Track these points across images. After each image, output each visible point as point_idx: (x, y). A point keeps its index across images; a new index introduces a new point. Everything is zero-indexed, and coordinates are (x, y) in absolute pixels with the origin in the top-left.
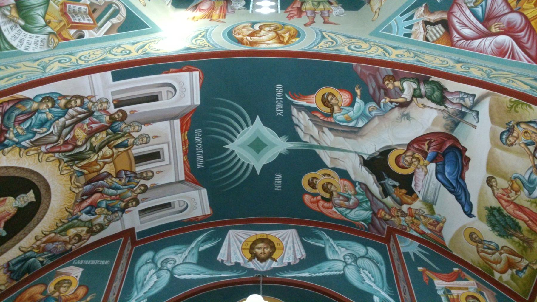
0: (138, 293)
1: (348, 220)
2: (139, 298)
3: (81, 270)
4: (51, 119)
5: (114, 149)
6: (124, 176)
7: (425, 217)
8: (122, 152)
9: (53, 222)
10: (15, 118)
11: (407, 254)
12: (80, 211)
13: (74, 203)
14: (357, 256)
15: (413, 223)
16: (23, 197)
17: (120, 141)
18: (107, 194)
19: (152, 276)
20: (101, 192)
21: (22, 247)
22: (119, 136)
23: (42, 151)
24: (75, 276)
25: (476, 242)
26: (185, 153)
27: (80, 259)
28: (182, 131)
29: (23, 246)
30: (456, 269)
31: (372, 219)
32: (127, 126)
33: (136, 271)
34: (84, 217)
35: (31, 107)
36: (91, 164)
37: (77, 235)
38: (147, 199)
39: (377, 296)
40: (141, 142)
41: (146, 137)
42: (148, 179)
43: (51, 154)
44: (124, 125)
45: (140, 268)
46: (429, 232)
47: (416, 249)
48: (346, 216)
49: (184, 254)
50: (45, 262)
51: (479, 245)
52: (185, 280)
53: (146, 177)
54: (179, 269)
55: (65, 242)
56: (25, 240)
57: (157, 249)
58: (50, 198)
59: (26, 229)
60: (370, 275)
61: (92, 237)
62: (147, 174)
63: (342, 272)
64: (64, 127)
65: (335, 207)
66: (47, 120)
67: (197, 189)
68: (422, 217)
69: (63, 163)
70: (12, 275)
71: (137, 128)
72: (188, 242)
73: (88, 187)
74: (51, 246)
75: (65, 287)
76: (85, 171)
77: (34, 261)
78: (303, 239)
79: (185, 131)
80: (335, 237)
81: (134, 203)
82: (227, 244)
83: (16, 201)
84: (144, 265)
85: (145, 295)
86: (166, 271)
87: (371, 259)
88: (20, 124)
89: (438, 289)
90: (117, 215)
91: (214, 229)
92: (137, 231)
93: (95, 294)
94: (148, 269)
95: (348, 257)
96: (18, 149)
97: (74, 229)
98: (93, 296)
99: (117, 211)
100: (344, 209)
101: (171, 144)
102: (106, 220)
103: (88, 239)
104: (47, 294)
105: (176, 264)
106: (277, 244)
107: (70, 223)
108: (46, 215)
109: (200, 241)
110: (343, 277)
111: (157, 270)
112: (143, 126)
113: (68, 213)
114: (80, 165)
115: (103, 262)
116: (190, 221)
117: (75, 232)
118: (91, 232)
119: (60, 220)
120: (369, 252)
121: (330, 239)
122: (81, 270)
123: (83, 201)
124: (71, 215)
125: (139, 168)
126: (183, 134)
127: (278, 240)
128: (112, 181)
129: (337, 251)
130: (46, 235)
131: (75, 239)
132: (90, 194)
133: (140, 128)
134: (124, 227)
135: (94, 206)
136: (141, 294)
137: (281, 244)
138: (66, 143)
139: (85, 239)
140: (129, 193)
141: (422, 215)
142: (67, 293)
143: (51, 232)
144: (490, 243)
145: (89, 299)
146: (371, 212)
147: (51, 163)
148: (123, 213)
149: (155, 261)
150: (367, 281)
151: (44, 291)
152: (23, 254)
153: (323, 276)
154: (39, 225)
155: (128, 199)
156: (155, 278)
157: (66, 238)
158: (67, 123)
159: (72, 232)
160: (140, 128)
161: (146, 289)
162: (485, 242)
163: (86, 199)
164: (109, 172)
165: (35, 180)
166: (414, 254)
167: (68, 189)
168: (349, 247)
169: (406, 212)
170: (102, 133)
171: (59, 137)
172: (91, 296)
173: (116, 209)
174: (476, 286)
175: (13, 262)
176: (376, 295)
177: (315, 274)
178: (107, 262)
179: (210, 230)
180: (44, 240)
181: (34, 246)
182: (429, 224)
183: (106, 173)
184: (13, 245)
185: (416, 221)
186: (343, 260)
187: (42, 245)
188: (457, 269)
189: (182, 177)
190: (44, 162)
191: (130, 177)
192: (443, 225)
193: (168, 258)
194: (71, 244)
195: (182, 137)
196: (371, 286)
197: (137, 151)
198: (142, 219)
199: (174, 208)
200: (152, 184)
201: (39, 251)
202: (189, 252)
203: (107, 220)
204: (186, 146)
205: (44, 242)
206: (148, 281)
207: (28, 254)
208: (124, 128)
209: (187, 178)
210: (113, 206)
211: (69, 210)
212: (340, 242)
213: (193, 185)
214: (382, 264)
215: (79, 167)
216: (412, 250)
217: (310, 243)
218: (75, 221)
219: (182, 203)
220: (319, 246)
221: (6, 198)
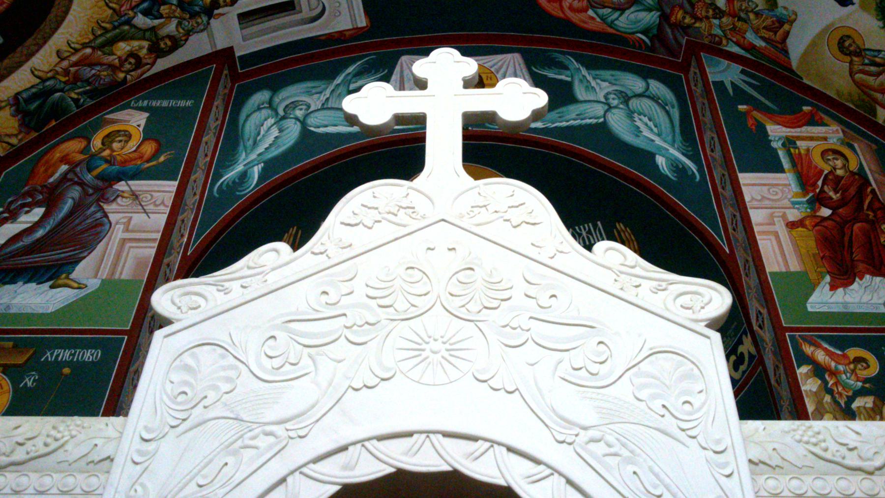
0: (247, 155)
1: (614, 32)
2: (249, 163)
3: (147, 115)
7: (758, 15)
9: (85, 27)
11: (720, 85)
12: (132, 9)
14: (630, 94)
15: (734, 29)
19: (269, 129)
21: (36, 69)
24: (135, 125)
25: (850, 54)
27: (143, 98)
29: (38, 68)
30: (806, 108)
31: (660, 27)
34: (141, 20)
37: (132, 54)
39: (663, 156)
45: (248, 116)
46: (763, 44)
47: (736, 77)
48: (611, 25)
50: (82, 100)
51: (855, 59)
52: (327, 134)
54: (316, 118)
55: (111, 66)
56: (38, 55)
57: (275, 86)
60: (651, 124)
61: (159, 60)
63: (601, 120)
65: (593, 7)
68: (752, 16)
70: (27, 119)
74: (88, 72)
75: (120, 141)
77: (62, 99)
78: (534, 69)
80: (591, 65)
82: (399, 79)
85: (260, 157)
86: (294, 120)
87: (654, 99)
89: (773, 139)
90: (199, 20)
91: (374, 54)
92: (238, 53)
94: (263, 117)
95: (612, 96)
97: (126, 43)
98: (170, 154)
100: (610, 10)
102: (181, 31)
104: (90, 153)
105: (311, 110)
106: (487, 77)
107: (117, 30)
108: (71, 12)
109: (349, 73)
110: (601, 130)
111: (278, 119)
113: (110, 12)
115: (182, 103)
116: (331, 39)
117: (128, 48)
118: (157, 51)
119: (98, 22)
120: (650, 87)
121: (581, 68)
122: (147, 115)
124: (117, 15)
127: (489, 71)
129: (593, 87)
130: (76, 51)
131: (130, 63)
134: (215, 46)
136: (253, 156)
137: (493, 77)
139: (147, 64)
141: (752, 11)
142: (123, 151)
143: (85, 46)
144: (876, 54)
146: (658, 13)
148: (210, 19)
149: (275, 105)
150: (646, 133)
151: (85, 148)
152: (40, 83)
153: (567, 127)
154: (61, 30)
156: (275, 132)
157: (113, 59)
159: (123, 48)
161: (261, 149)
162: (868, 53)
166: (732, 83)
168: (615, 80)
169: (724, 9)
172: (165, 154)
173: (197, 9)
174: (841, 135)
175: (25, 95)
176: (660, 155)
177: (553, 123)
178: (189, 103)
179: (370, 55)
180: (74, 58)
181: (57, 68)
182: (764, 28)
184: (19, 65)
185: (739, 24)
186: (603, 100)
187: (72, 69)
188: (809, 108)
192: (790, 29)
193: (297, 101)
194: (123, 72)
196: (653, 141)
198: (248, 31)
199: (301, 12)
201: (67, 81)
202: (333, 91)
203: (183, 29)
205: (75, 64)
206: (263, 136)
211: (111, 5)
212: (598, 72)
214: (673, 107)
216: (730, 79)
217: (546, 76)
218: (126, 27)
220: (561, 80)
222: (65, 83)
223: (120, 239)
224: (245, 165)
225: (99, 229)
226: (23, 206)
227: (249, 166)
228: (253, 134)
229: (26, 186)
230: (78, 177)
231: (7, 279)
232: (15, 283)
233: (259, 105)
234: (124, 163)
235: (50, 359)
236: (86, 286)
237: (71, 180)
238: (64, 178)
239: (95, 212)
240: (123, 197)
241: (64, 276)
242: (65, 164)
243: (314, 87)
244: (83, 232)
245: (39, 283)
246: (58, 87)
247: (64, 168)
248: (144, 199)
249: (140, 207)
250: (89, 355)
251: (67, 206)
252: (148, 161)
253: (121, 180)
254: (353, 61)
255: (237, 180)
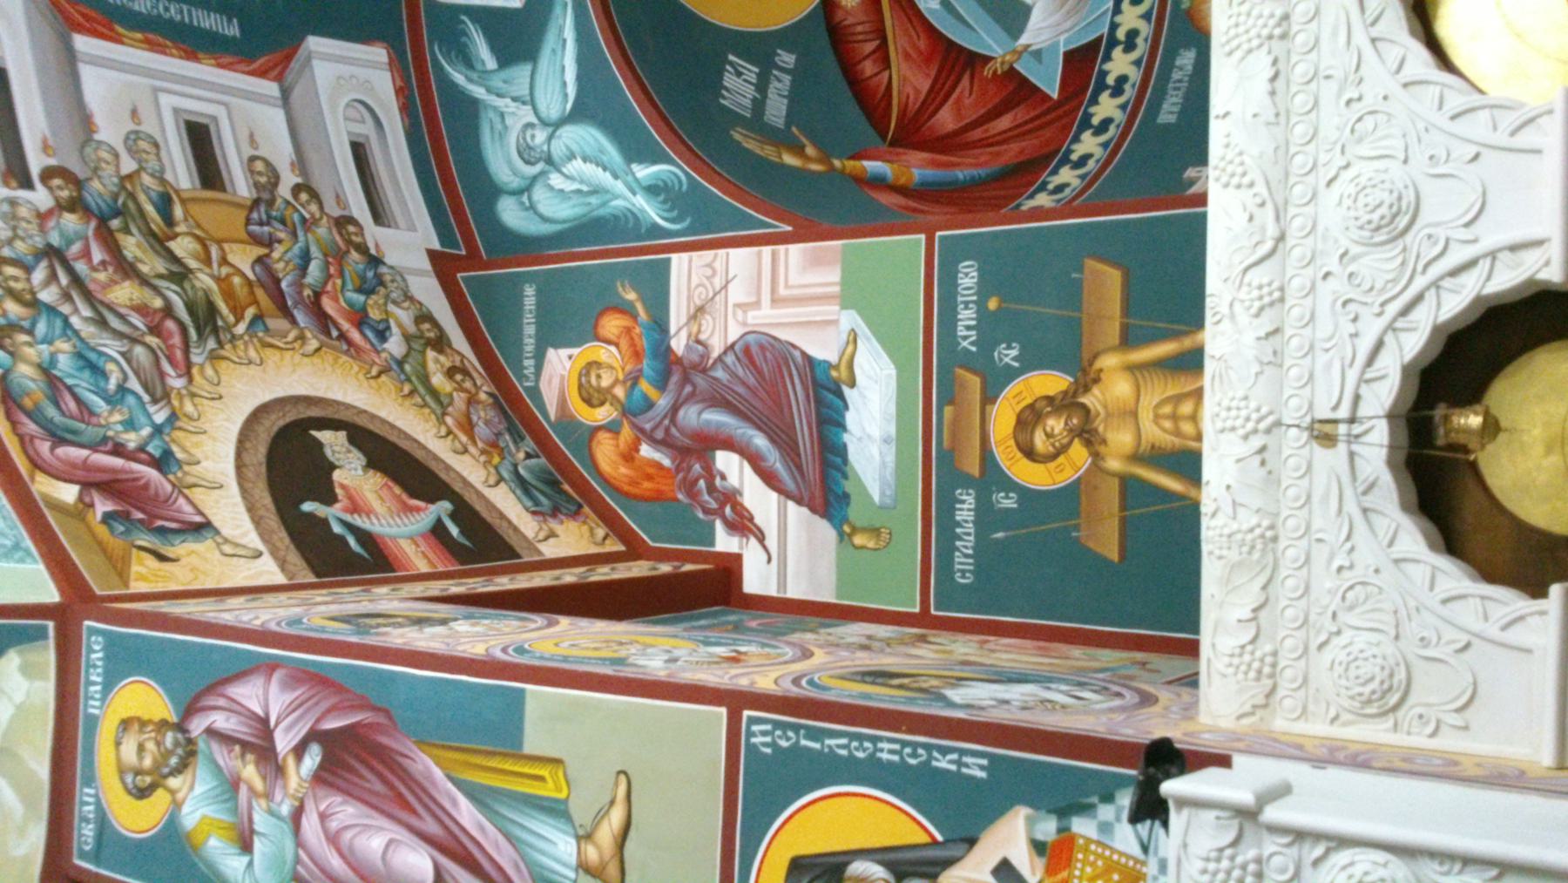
0: (616, 197)
3: (551, 353)
4: (75, 347)
5: (178, 229)
6: (266, 229)
8: (186, 212)
10: (72, 417)
13: (352, 357)
16: (333, 452)
17: (150, 209)
18: (326, 283)
20: (317, 295)
21: (486, 481)
22: (131, 205)
23: (185, 388)
24: (568, 364)
26: (191, 56)
28: (117, 40)
29: (483, 479)
32: (99, 177)
33: (559, 227)
34: (395, 345)
35: (33, 380)
36: (229, 295)
38: (338, 197)
40: (152, 157)
41: (135, 140)
42: (275, 180)
43: (195, 371)
44: (96, 184)
49: (505, 110)
52: (579, 78)
53: (269, 177)
55: (472, 401)
57: (491, 191)
58: (335, 401)
59: (433, 465)
61: (455, 346)
62: (260, 173)
64: (102, 323)
66: (79, 355)
67: (309, 59)
69: (223, 353)
71: (104, 155)
72: (468, 111)
73: (300, 316)
76: (250, 312)
77: (527, 468)
79: (112, 30)
81: (351, 229)
83: (347, 466)
84: (536, 213)
85: (620, 173)
86: (553, 142)
88: (92, 413)
93: (619, 284)
96: (178, 434)
98: (623, 286)
99: (375, 273)
101: (158, 83)
103: (459, 353)
105: (535, 120)
109: (466, 77)
111: (551, 168)
112: (97, 137)
113: (384, 378)
114: (231, 319)
116: (406, 109)
118: (440, 343)
123: (343, 336)
125: (242, 186)
126: (125, 40)
128: (280, 259)
132: (323, 321)
133: (104, 147)
135: (360, 318)
136: (619, 186)
138: (155, 330)
139: (462, 361)
140: (322, 231)
142: (616, 365)
145: (631, 296)
147: (224, 378)
148: (384, 264)
149: (523, 184)
155: (338, 238)
156: (576, 167)
158: (87, 312)
159: (438, 380)
160: (104, 147)
163: (339, 329)
164: (250, 261)
165: (279, 418)
167: (306, 360)
170: (122, 243)
171: (135, 341)
172: (623, 294)
173: (370, 274)
175: (529, 504)
178: (530, 291)
183: (258, 269)
187: (480, 445)
189: (271, 88)
190: (220, 389)
191: (269, 217)
195: (132, 46)
197: (182, 174)
200: (293, 171)
204: (167, 46)
206: (582, 182)
207: (505, 475)
208: (104, 185)
209: (275, 72)
210: (363, 279)
213: (295, 65)
215: (238, 321)
218: (407, 368)
219: (352, 113)
221: (336, 485)
222: (503, 458)
223: (772, 307)
224: (634, 194)
225: (755, 350)
226: (711, 489)
227: (637, 189)
228: (582, 200)
229: (676, 500)
230: (661, 422)
231: (838, 460)
232: (845, 446)
233: (527, 209)
234: (637, 355)
235: (974, 338)
236: (853, 330)
237: (667, 430)
238: (664, 443)
239: (726, 368)
240: (699, 331)
241: (834, 374)
242: (637, 450)
243: (492, 128)
244: (758, 371)
245: (846, 407)
246: (511, 468)
247: (646, 451)
248: (703, 297)
249: (717, 298)
250: (968, 277)
251: (716, 418)
252: (634, 317)
253: (669, 349)
254: (445, 81)
255: (661, 198)
